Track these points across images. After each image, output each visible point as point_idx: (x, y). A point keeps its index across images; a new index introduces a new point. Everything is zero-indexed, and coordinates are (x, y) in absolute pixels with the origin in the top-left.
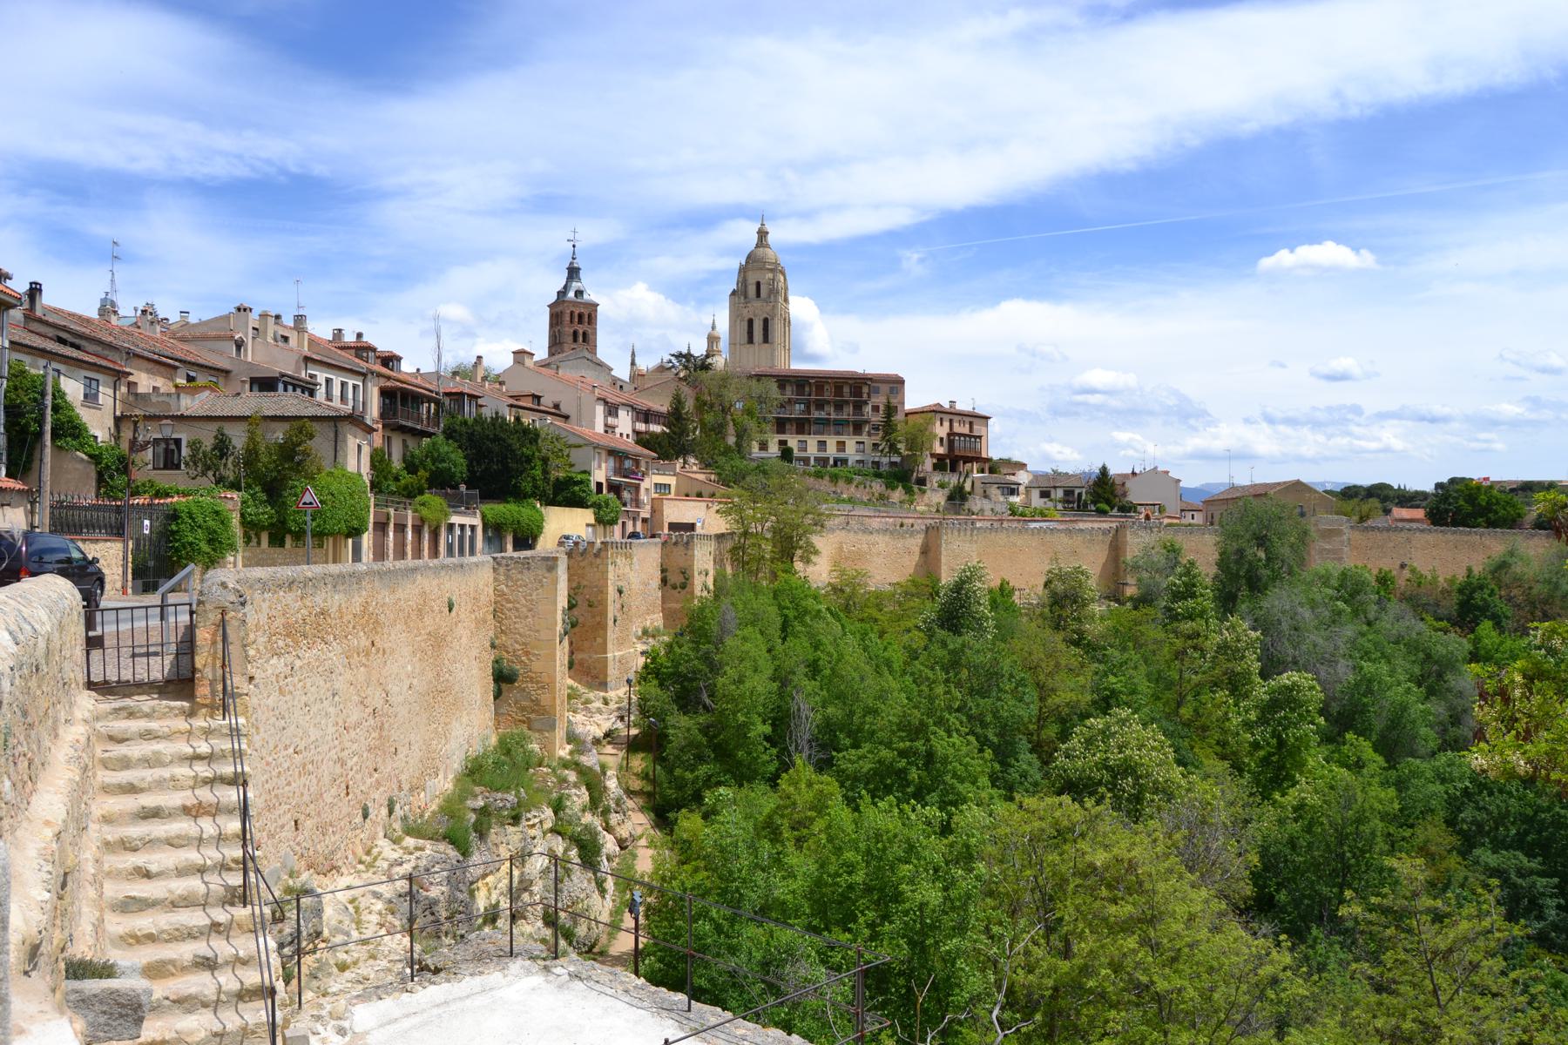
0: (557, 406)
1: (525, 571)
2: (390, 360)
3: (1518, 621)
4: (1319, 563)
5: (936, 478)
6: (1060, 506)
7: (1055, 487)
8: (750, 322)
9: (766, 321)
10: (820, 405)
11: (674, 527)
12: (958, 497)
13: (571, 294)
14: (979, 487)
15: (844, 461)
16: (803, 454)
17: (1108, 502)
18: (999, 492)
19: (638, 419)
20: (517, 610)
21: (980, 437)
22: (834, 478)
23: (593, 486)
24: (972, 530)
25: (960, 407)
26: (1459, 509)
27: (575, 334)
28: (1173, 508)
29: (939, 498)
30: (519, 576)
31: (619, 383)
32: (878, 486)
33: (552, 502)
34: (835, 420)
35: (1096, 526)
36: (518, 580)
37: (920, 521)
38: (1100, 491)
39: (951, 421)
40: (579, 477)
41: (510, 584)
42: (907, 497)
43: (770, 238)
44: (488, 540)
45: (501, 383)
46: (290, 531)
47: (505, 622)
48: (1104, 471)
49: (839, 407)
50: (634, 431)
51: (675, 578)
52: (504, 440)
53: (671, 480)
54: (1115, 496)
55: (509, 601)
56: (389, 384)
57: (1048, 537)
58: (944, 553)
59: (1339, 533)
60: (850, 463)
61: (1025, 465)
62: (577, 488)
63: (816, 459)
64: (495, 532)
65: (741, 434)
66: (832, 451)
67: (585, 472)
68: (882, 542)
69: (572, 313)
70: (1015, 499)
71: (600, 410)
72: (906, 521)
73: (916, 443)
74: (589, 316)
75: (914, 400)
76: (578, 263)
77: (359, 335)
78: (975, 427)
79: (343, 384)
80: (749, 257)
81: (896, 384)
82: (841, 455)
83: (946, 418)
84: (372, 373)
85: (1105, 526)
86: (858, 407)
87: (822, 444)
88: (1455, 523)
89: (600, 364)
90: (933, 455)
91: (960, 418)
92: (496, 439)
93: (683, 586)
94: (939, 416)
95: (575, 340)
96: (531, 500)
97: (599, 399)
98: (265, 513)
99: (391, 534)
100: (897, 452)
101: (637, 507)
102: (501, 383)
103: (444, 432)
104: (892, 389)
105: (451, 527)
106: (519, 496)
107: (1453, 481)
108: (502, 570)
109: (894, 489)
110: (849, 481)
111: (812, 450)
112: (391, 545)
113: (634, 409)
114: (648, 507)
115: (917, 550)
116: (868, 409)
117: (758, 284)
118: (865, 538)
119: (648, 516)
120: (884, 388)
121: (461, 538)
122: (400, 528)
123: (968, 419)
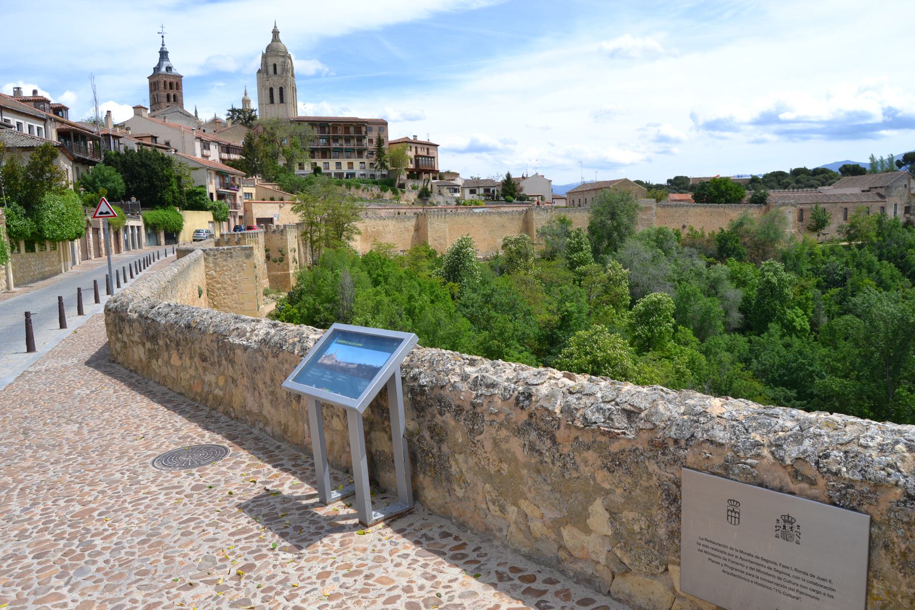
0: (167, 144)
1: (229, 259)
2: (60, 110)
3: (751, 256)
4: (640, 229)
5: (410, 184)
6: (483, 198)
7: (479, 187)
8: (271, 90)
9: (281, 89)
10: (336, 140)
11: (260, 221)
12: (424, 195)
13: (163, 70)
14: (435, 188)
15: (353, 175)
16: (327, 171)
17: (512, 195)
18: (448, 191)
19: (223, 151)
20: (225, 289)
21: (434, 157)
22: (349, 186)
23: (208, 195)
24: (445, 215)
25: (420, 139)
26: (711, 193)
27: (168, 96)
28: (548, 198)
29: (412, 196)
30: (225, 263)
31: (202, 128)
32: (376, 190)
33: (187, 209)
34: (346, 149)
35: (515, 209)
36: (224, 266)
37: (409, 210)
38: (507, 188)
39: (416, 148)
40: (199, 190)
41: (218, 269)
42: (394, 196)
44: (148, 236)
45: (127, 129)
46: (46, 238)
47: (216, 298)
48: (508, 176)
49: (348, 140)
51: (275, 255)
52: (149, 166)
53: (252, 190)
54: (515, 191)
55: (218, 283)
56: (63, 127)
57: (488, 217)
58: (429, 230)
59: (650, 208)
60: (357, 176)
61: (458, 174)
62: (198, 198)
63: (335, 174)
64: (152, 229)
65: (290, 159)
66: (345, 169)
67: (202, 186)
68: (391, 224)
69: (165, 82)
70: (458, 195)
71: (198, 145)
72: (401, 211)
73: (397, 161)
74: (177, 84)
75: (393, 134)
76: (168, 48)
77: (35, 92)
78: (430, 151)
79: (30, 127)
80: (269, 48)
81: (382, 125)
82: (351, 171)
83: (414, 146)
84: (51, 119)
85: (520, 209)
86: (360, 139)
87: (339, 165)
88: (708, 202)
89: (189, 116)
91: (421, 146)
92: (144, 165)
93: (281, 260)
95: (168, 100)
96: (173, 207)
97: (197, 138)
98: (25, 224)
99: (91, 235)
100: (386, 168)
101: (235, 208)
102: (127, 129)
103: (104, 162)
104: (380, 128)
105: (126, 228)
106: (164, 204)
107: (677, 178)
108: (211, 259)
109: (385, 191)
110: (358, 187)
111: (333, 169)
112: (92, 244)
113: (219, 144)
114: (242, 209)
115: (412, 229)
116: (366, 141)
117: (275, 66)
118: (380, 222)
119: (242, 214)
120: (375, 128)
121: (132, 235)
122: (96, 231)
123: (426, 147)
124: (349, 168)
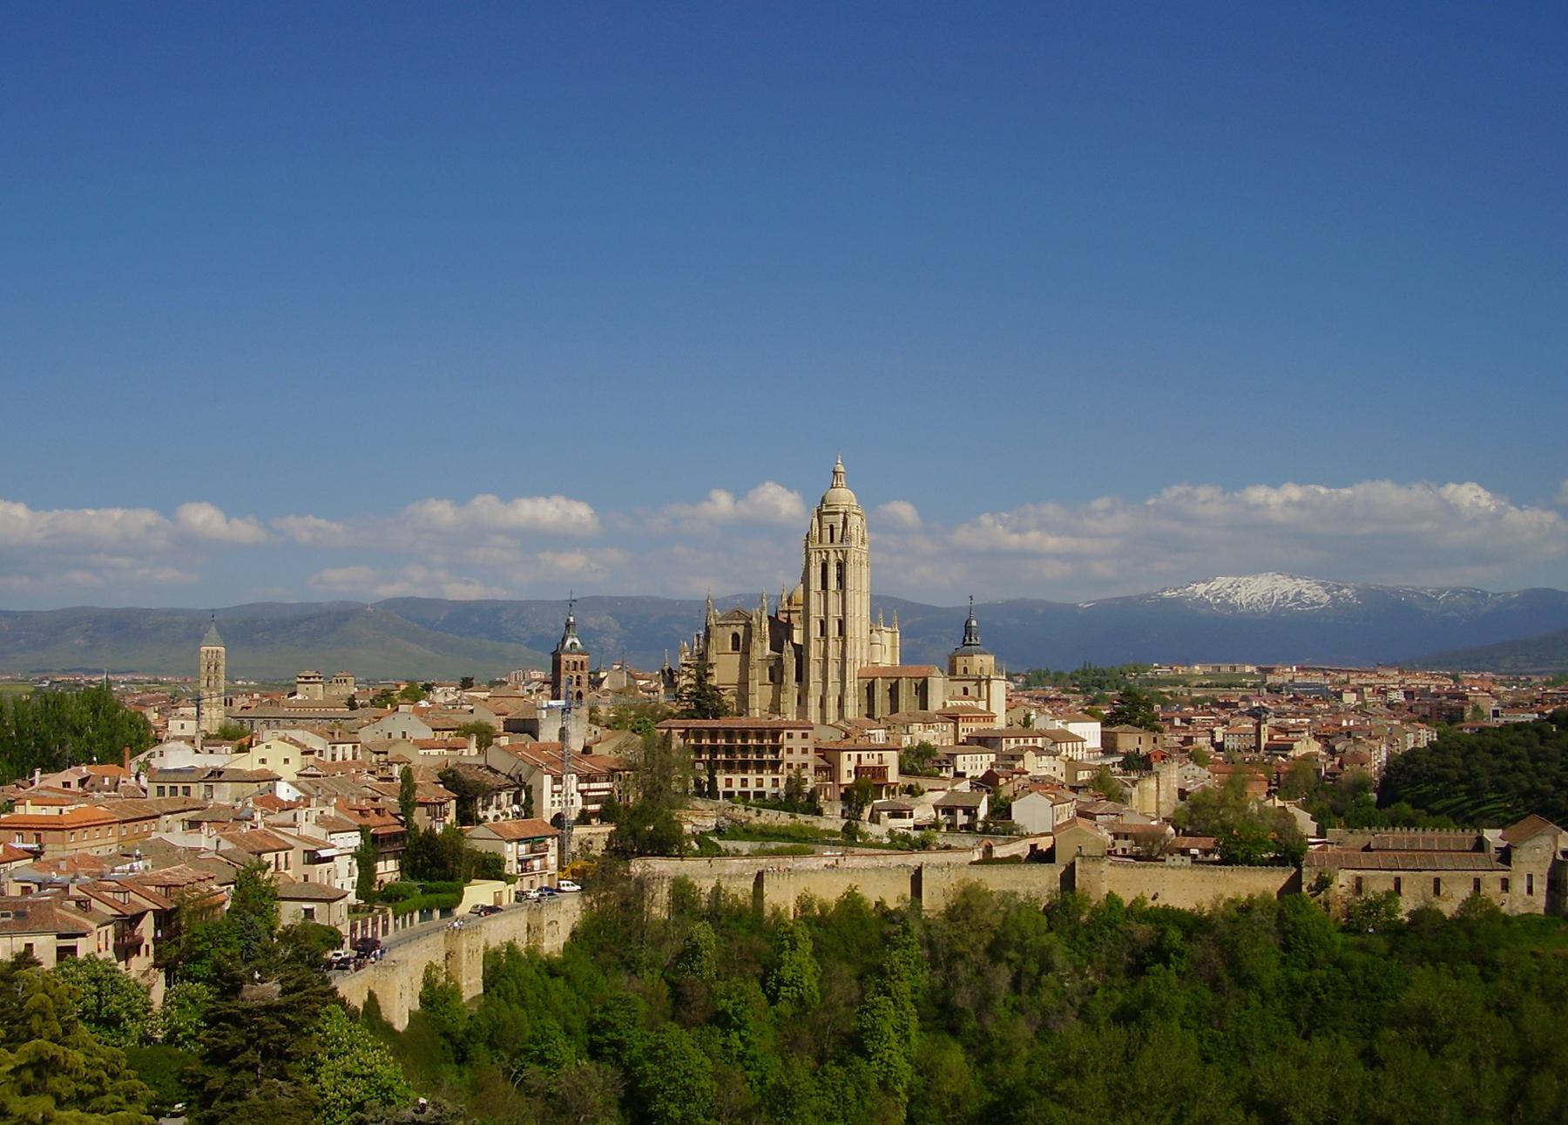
39: (859, 756)
49: (759, 750)
63: (739, 792)
71: (548, 779)
87: (744, 782)
111: (736, 787)
117: (832, 527)
123: (876, 753)
124: (758, 786)
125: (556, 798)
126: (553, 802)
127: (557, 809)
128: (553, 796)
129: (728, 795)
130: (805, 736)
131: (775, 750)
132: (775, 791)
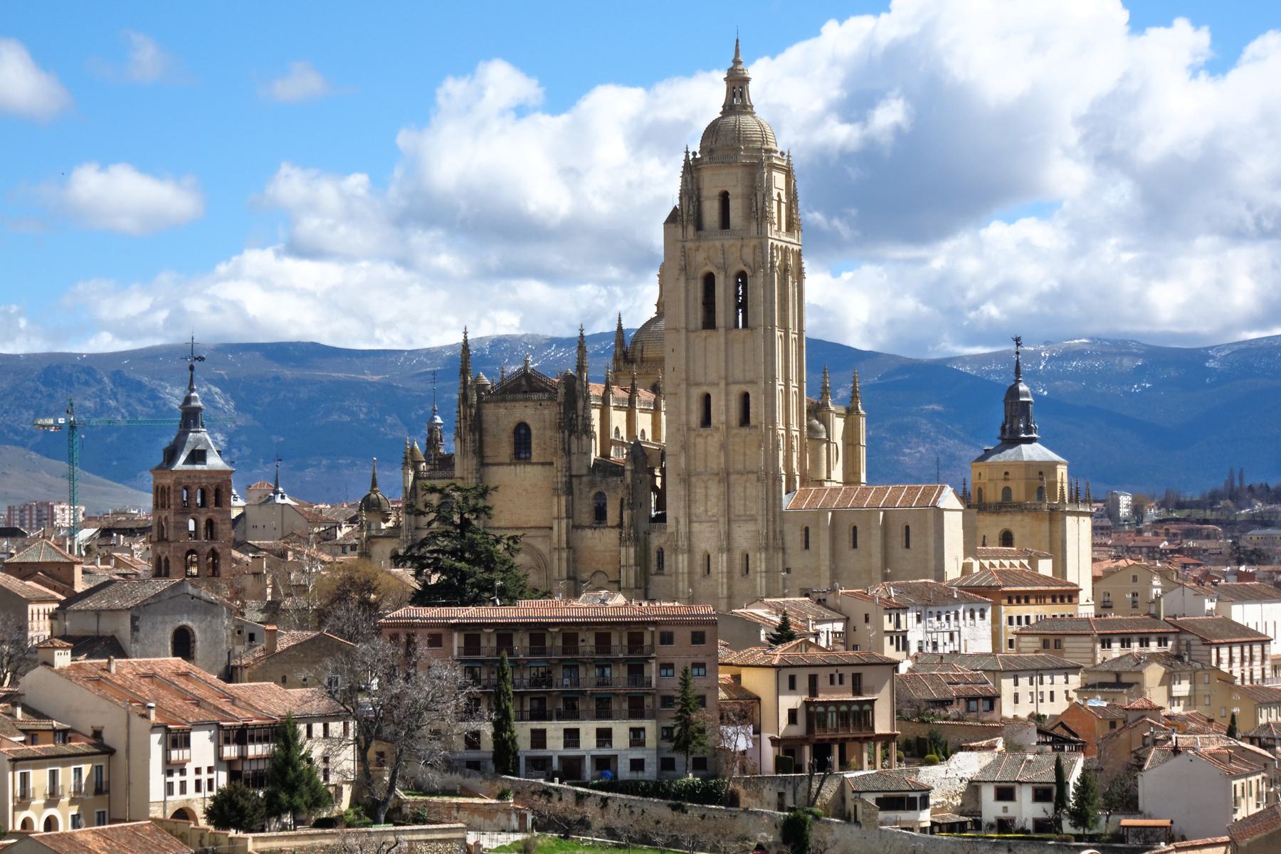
7: (1020, 783)
19: (227, 742)
39: (813, 680)
43: (755, 91)
50: (219, 757)
63: (560, 758)
71: (156, 738)
80: (713, 131)
87: (572, 737)
90: (774, 742)
91: (832, 671)
94: (785, 674)
117: (725, 198)
125: (176, 779)
126: (169, 789)
127: (177, 799)
128: (169, 773)
129: (540, 765)
130: (698, 638)
131: (636, 670)
132: (637, 754)
